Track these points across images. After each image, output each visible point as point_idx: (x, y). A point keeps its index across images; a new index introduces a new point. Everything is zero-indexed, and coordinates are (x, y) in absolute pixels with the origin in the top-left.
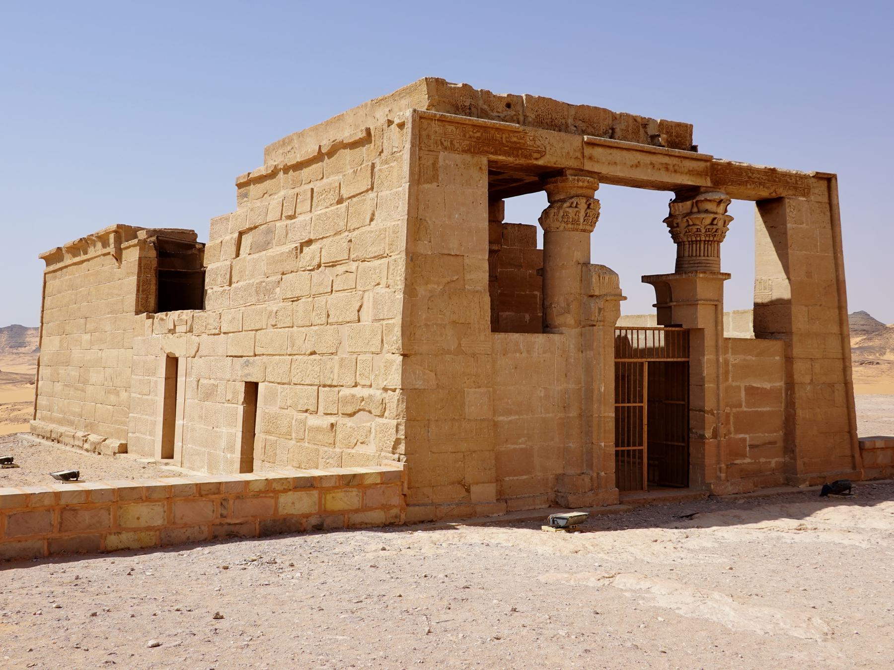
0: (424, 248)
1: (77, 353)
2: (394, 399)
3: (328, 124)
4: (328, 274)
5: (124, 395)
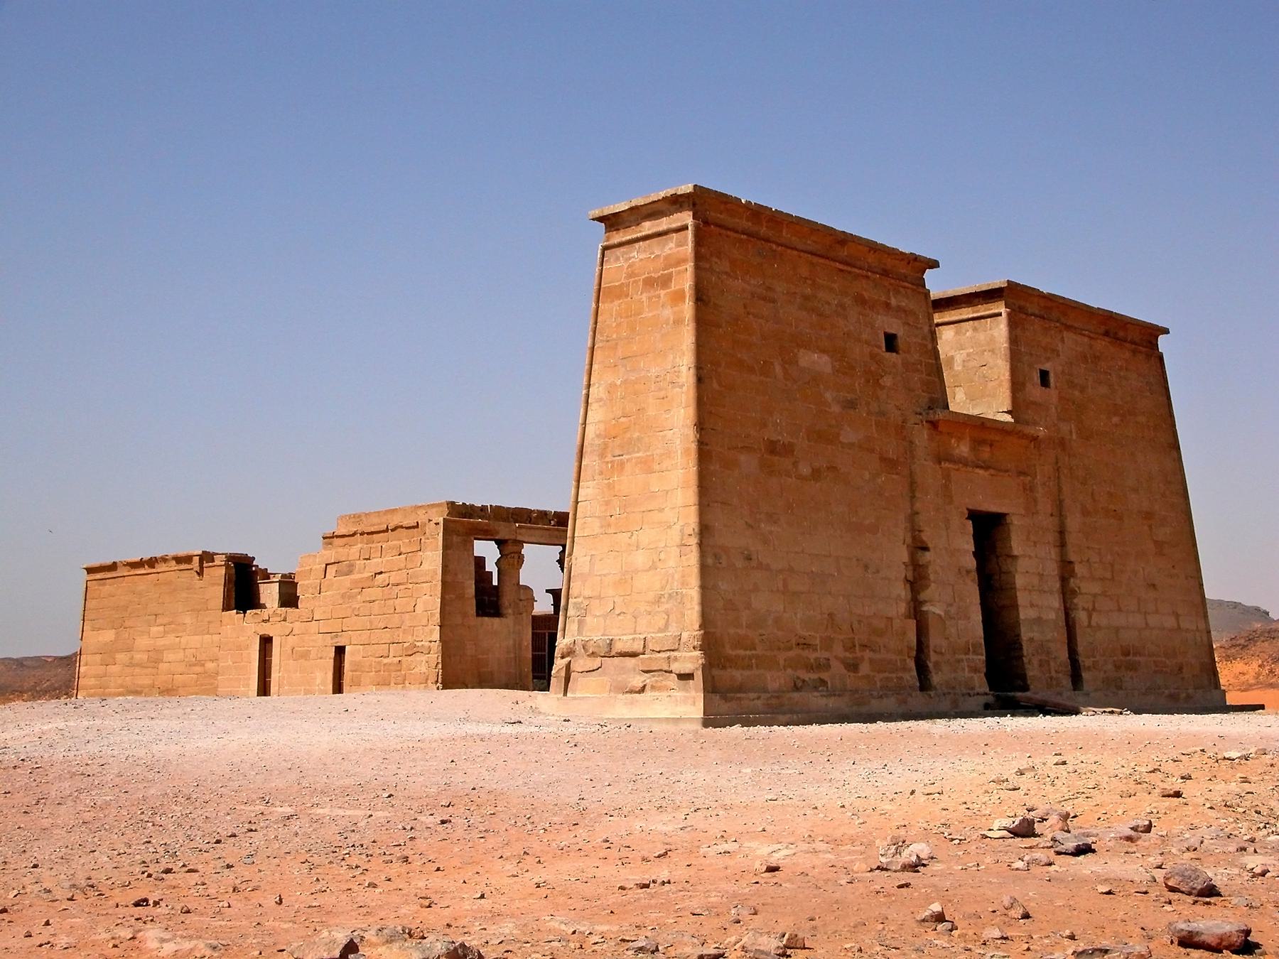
0: (449, 578)
1: (143, 642)
2: (436, 647)
3: (387, 512)
4: (396, 589)
5: (210, 665)
